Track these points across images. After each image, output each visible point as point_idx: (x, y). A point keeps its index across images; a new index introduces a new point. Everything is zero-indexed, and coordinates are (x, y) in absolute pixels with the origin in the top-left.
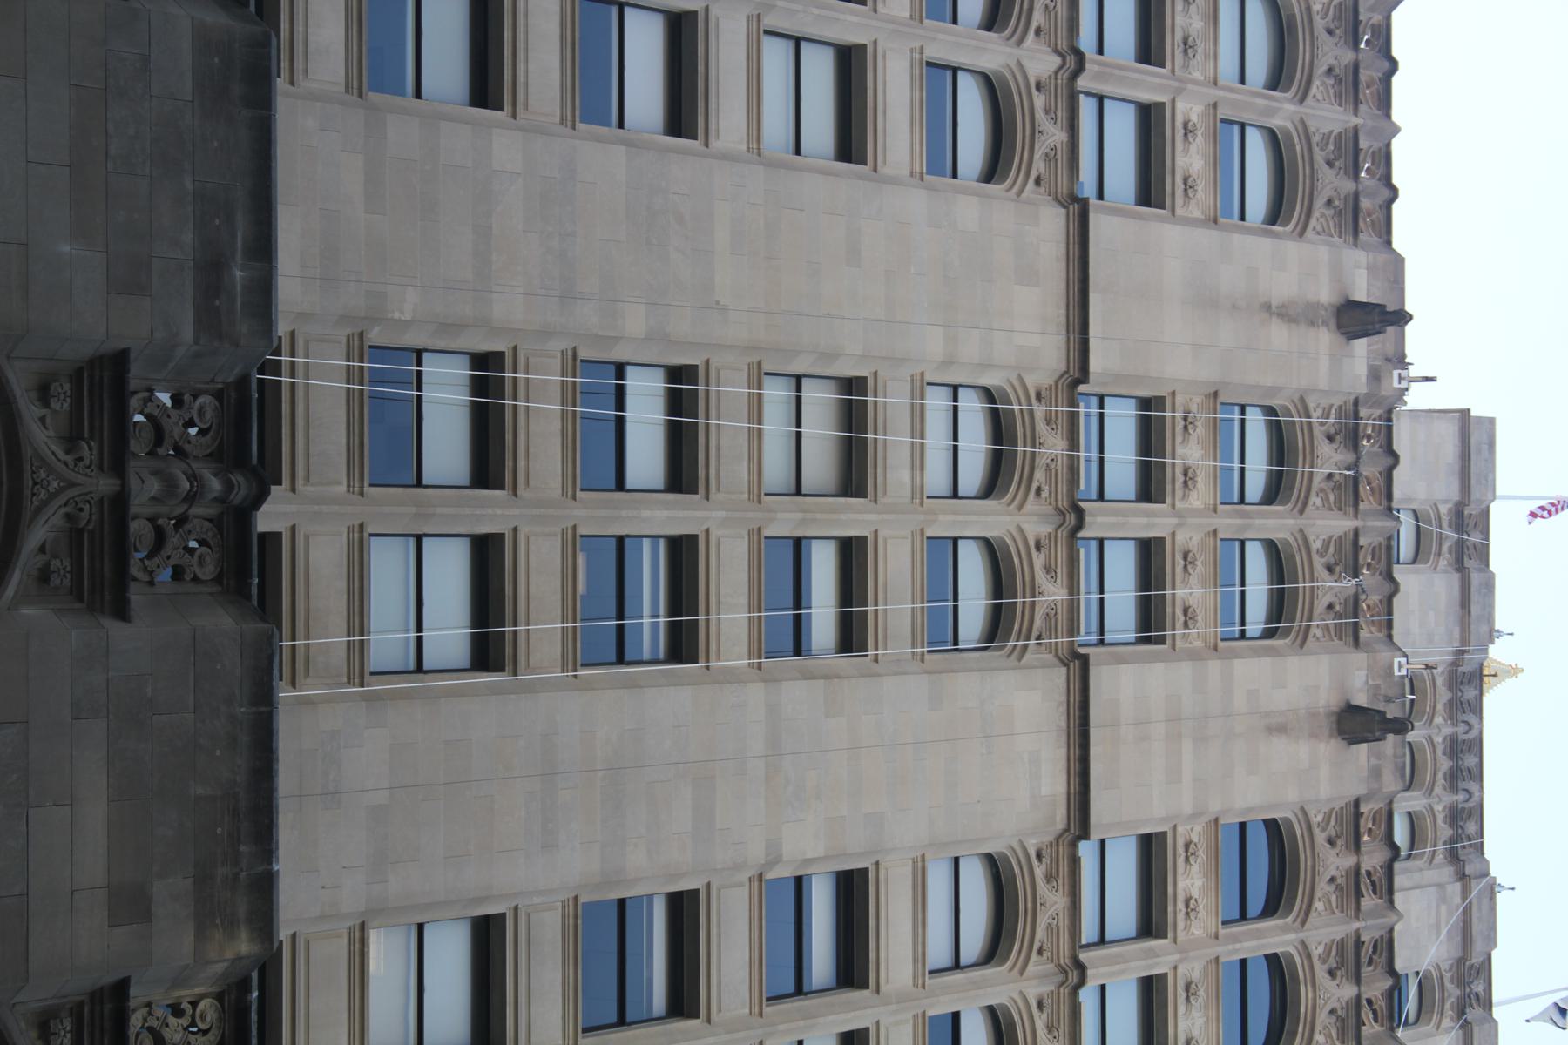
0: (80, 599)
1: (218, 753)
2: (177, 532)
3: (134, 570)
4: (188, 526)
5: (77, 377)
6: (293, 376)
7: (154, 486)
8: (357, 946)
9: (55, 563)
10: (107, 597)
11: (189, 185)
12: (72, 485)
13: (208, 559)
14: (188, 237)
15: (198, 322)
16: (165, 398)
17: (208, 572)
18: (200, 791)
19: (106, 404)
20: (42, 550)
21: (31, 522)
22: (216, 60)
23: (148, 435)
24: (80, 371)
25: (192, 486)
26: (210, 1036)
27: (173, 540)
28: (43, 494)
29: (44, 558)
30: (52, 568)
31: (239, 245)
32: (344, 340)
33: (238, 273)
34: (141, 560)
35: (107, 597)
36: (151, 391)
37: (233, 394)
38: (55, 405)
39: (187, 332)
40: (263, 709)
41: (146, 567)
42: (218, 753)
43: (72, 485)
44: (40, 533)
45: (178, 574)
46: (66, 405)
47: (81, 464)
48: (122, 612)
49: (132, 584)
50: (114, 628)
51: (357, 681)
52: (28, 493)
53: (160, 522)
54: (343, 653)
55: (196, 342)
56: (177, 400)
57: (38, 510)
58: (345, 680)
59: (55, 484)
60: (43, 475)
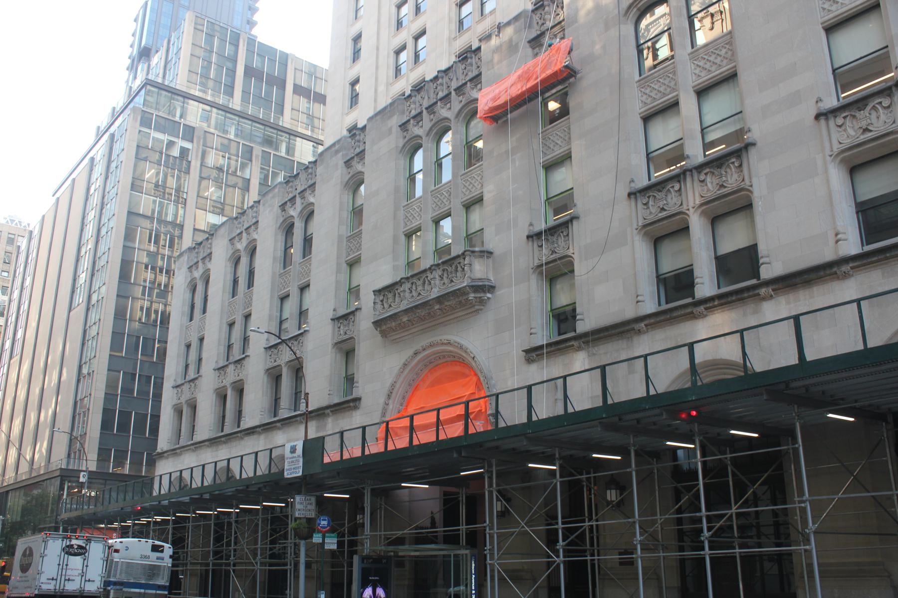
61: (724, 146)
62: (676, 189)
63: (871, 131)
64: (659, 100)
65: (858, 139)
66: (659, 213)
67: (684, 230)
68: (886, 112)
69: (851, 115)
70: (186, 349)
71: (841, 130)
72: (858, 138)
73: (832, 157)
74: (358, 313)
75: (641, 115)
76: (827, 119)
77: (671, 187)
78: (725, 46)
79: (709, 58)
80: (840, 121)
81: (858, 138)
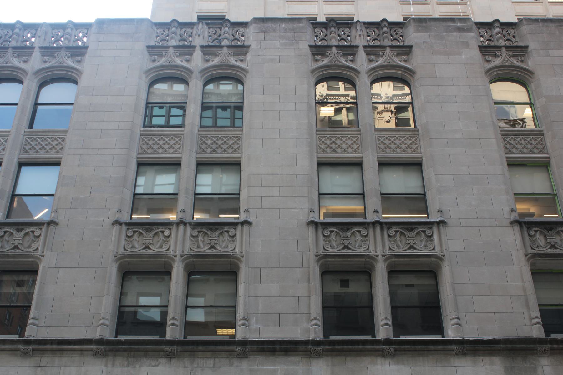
0: (525, 55)
1: (550, 29)
2: (506, 37)
3: (349, 44)
4: (340, 34)
5: (484, 55)
6: (411, 15)
7: (501, 41)
8: (516, 3)
9: (520, 59)
10: (524, 50)
11: (445, 34)
12: (505, 56)
13: (510, 31)
14: (455, 34)
15: (470, 32)
16: (368, 38)
17: (512, 31)
18: (557, 32)
19: (488, 50)
20: (518, 61)
21: (514, 63)
22: (420, 28)
23: (376, 41)
24: (483, 54)
25: (499, 34)
26: (487, 31)
27: (342, 37)
28: (509, 61)
29: (519, 61)
30: (520, 60)
31: (453, 24)
32: (401, 5)
33: (459, 25)
34: (347, 43)
35: (524, 50)
36: (368, 41)
37: (478, 26)
38: (490, 59)
39: (473, 34)
40: (539, 20)
41: (515, 43)
42: (550, 29)
43: (505, 56)
44: (515, 62)
45: (349, 36)
46: (490, 57)
47: (501, 54)
48: (527, 47)
49: (404, 45)
50: (529, 49)
51: (466, 3)
52: (509, 64)
53: (505, 40)
54: (461, 6)
55: (474, 33)
56: (369, 36)
57: (512, 62)
58: (466, 5)
59: (506, 59)
60: (505, 61)
61: (557, 215)
62: (36, 235)
63: (557, 248)
64: (149, 154)
65: (339, 251)
66: (208, 249)
67: (169, 273)
68: (230, 240)
69: (540, 231)
70: (17, 167)
71: (194, 240)
72: (547, 250)
73: (528, 256)
74: (52, 227)
75: (19, 160)
76: (521, 227)
77: (31, 231)
78: (58, 139)
79: (41, 142)
80: (327, 233)
81: (547, 250)
